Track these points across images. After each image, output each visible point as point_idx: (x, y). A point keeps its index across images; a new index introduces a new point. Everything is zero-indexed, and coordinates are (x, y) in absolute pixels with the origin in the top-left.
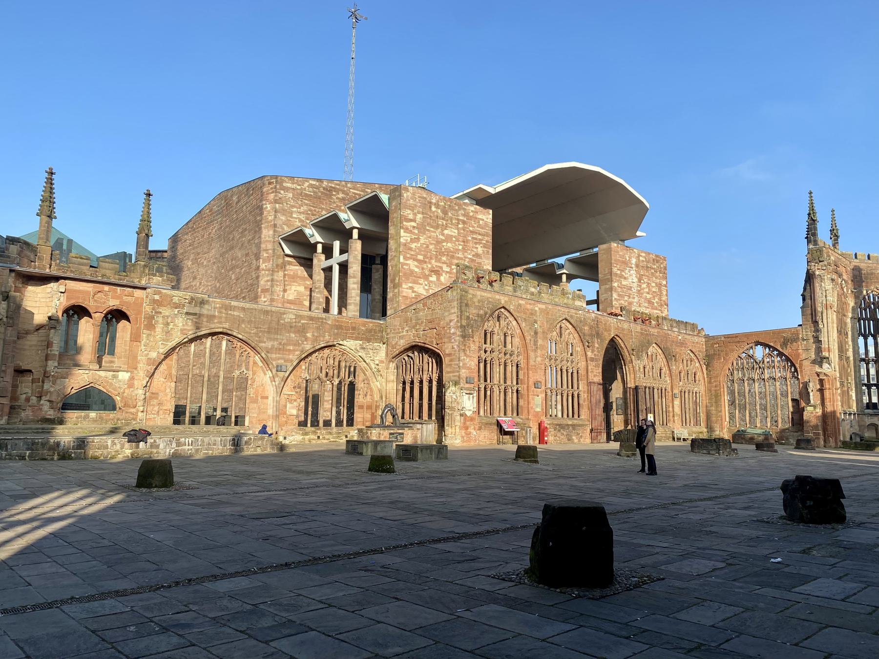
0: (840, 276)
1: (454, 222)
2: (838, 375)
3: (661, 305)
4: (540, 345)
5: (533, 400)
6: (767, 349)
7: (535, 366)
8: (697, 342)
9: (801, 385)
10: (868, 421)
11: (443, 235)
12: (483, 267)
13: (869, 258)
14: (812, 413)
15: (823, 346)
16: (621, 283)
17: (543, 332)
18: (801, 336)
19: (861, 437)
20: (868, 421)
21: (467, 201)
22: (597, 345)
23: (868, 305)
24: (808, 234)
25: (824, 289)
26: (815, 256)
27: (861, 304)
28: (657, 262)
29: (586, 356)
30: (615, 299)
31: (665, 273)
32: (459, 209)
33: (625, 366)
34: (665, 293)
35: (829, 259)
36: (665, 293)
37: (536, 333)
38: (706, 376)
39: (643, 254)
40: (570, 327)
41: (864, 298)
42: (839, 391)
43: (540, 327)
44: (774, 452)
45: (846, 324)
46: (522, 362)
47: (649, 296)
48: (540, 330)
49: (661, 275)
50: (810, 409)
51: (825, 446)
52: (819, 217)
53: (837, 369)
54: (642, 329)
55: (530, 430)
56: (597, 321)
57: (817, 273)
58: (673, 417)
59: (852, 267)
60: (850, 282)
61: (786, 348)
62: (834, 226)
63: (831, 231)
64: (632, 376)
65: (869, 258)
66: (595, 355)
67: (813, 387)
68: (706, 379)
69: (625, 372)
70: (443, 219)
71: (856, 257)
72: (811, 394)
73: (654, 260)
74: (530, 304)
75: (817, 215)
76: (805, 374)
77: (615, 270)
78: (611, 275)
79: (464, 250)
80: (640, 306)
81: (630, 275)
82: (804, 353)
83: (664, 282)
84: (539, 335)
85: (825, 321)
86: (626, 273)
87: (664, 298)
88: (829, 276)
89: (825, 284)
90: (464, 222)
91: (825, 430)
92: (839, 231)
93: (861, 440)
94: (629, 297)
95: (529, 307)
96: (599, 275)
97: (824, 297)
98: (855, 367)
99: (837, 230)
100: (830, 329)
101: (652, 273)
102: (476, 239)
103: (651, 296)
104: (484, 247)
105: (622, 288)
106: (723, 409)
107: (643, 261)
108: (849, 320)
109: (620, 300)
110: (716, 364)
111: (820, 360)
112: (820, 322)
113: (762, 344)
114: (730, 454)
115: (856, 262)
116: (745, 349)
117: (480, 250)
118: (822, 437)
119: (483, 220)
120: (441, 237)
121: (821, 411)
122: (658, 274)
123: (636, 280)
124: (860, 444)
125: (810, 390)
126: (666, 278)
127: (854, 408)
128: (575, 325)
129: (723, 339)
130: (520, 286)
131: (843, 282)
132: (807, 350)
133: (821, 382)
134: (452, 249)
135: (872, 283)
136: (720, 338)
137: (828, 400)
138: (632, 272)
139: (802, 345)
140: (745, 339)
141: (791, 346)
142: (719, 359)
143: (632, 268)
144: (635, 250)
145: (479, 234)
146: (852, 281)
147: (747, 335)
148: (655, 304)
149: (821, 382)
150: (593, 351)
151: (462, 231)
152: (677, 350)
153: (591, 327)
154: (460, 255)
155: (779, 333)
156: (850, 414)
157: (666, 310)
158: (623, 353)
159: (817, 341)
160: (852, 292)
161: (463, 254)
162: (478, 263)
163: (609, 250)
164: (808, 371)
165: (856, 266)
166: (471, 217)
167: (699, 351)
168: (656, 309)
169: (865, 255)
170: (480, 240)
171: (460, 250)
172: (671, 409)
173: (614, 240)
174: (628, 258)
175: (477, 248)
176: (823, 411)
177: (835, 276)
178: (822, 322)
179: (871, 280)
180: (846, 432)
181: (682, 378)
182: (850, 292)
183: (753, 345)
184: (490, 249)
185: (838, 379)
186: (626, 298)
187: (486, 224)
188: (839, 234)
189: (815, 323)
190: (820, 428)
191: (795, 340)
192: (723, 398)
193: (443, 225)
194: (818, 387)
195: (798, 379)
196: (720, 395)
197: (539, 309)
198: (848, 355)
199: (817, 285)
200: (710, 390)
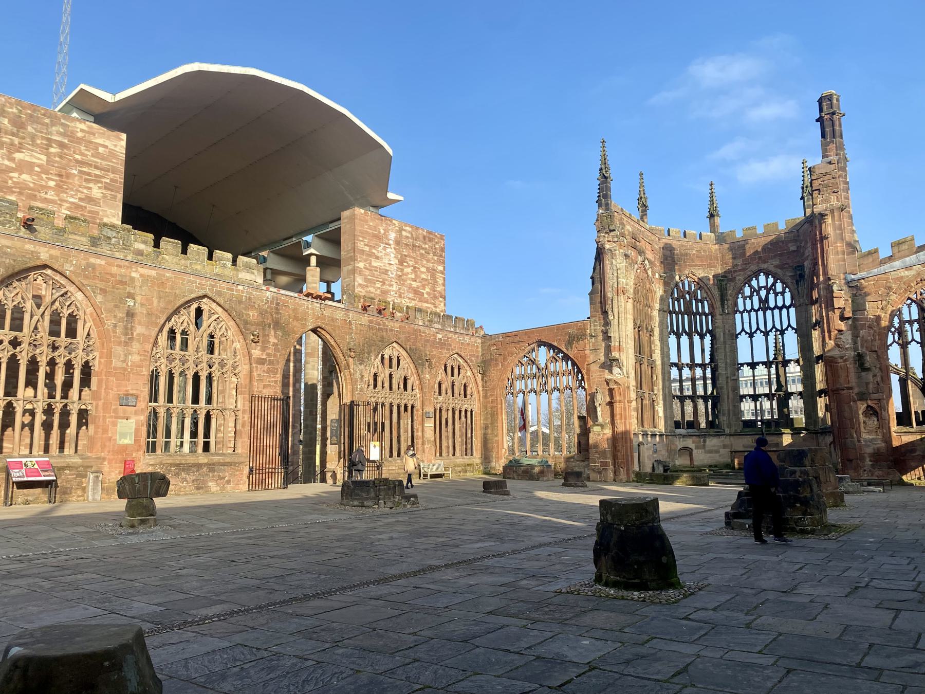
0: (641, 252)
1: (39, 142)
2: (633, 383)
3: (435, 297)
4: (138, 335)
5: (115, 424)
6: (552, 351)
7: (125, 369)
8: (468, 344)
9: (589, 397)
10: (680, 444)
11: (12, 160)
12: (102, 219)
13: (685, 236)
14: (600, 434)
15: (612, 344)
16: (370, 263)
17: (149, 314)
18: (588, 331)
19: (664, 466)
20: (680, 444)
21: (75, 115)
22: (273, 340)
23: (681, 294)
24: (599, 196)
25: (615, 268)
26: (605, 224)
27: (672, 294)
28: (430, 241)
29: (250, 355)
30: (360, 285)
31: (441, 256)
32: (53, 124)
33: (340, 373)
34: (440, 281)
35: (623, 228)
36: (440, 281)
37: (130, 314)
38: (481, 389)
39: (408, 228)
40: (219, 309)
41: (677, 285)
42: (634, 404)
43: (142, 305)
44: (505, 495)
45: (651, 318)
46: (96, 362)
47: (414, 284)
48: (139, 309)
49: (436, 258)
50: (596, 429)
51: (615, 480)
52: (613, 173)
53: (632, 375)
54: (370, 322)
55: (97, 477)
56: (278, 304)
57: (607, 246)
58: (423, 444)
59: (662, 245)
60: (658, 264)
61: (571, 348)
62: (642, 193)
63: (638, 200)
64: (349, 387)
65: (685, 236)
66: (268, 354)
67: (601, 399)
68: (481, 393)
69: (341, 383)
70: (13, 134)
71: (669, 235)
72: (599, 409)
73: (424, 237)
74: (119, 266)
75: (610, 171)
76: (593, 383)
77: (360, 245)
78: (354, 252)
79: (59, 188)
80: (400, 296)
81: (386, 254)
82: (594, 355)
83: (440, 268)
84: (136, 319)
85: (615, 310)
86: (380, 251)
87: (439, 288)
88: (621, 251)
89: (616, 261)
90: (61, 145)
91: (615, 458)
92: (648, 200)
93: (665, 471)
94: (384, 283)
95: (114, 270)
96: (342, 253)
97: (615, 278)
98: (663, 374)
99: (646, 198)
100: (622, 320)
101: (422, 254)
102: (89, 174)
103: (419, 284)
104: (106, 188)
105: (371, 270)
106: (500, 432)
107: (407, 237)
108: (656, 314)
109: (367, 287)
110: (494, 373)
111: (610, 363)
112: (610, 313)
113: (550, 346)
114: (397, 504)
115: (666, 240)
116: (527, 351)
117: (96, 192)
118: (611, 467)
119: (105, 147)
120: (6, 162)
121: (611, 431)
122: (431, 256)
123: (395, 261)
124: (658, 476)
125: (597, 404)
126: (444, 263)
127: (661, 427)
128: (227, 307)
129: (501, 339)
130: (109, 238)
131: (646, 262)
132: (596, 350)
133: (611, 391)
134: (31, 185)
135: (686, 266)
136: (498, 338)
137: (618, 416)
138: (388, 250)
139: (589, 343)
140: (525, 338)
141: (577, 346)
142: (497, 365)
143: (390, 245)
144: (394, 221)
145: (96, 167)
146: (662, 262)
147: (528, 333)
148: (426, 296)
149: (611, 391)
150: (264, 349)
151: (57, 159)
152: (434, 353)
153: (262, 313)
154: (51, 195)
155: (564, 329)
156: (654, 435)
157: (442, 304)
158: (335, 355)
159: (607, 338)
160: (661, 276)
161: (58, 195)
162: (90, 212)
163: (353, 218)
164: (597, 375)
165: (666, 244)
166: (78, 138)
167: (471, 355)
168: (427, 302)
169: (679, 231)
170: (96, 176)
171: (50, 187)
172: (420, 434)
173: (362, 206)
174: (382, 231)
175: (90, 188)
176: (613, 431)
177: (632, 253)
178: (612, 311)
179: (685, 262)
180: (647, 460)
181: (443, 391)
182: (657, 276)
183: (535, 345)
184: (118, 192)
185: (632, 388)
186: (378, 285)
187: (112, 154)
188: (648, 203)
189: (605, 313)
190: (609, 455)
191: (581, 338)
192: (500, 418)
193: (12, 144)
194: (608, 399)
195: (585, 389)
196: (497, 414)
197: (141, 275)
198: (653, 359)
199: (607, 262)
200: (486, 408)
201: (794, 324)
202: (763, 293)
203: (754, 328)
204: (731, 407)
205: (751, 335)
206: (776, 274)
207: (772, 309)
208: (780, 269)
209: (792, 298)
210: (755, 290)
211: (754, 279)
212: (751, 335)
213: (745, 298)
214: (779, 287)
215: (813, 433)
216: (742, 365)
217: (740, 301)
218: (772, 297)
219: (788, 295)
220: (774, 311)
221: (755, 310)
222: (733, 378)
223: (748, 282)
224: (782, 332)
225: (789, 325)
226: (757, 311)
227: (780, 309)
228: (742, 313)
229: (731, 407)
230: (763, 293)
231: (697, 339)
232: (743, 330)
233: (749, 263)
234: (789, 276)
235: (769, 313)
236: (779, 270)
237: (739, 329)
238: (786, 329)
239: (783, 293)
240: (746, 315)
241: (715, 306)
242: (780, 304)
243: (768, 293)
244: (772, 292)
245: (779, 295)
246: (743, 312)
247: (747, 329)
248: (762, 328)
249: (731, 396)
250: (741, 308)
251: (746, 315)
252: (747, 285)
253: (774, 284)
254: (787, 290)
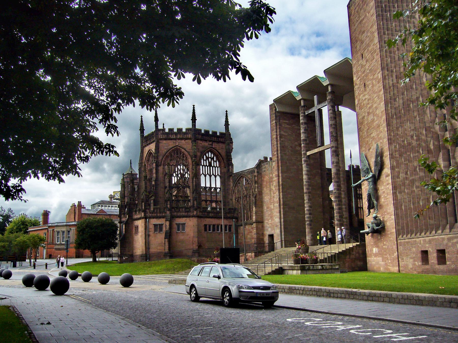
202: (210, 160)
209: (219, 164)
213: (204, 160)
218: (212, 162)
224: (215, 176)
225: (218, 174)
230: (210, 160)
232: (203, 173)
237: (201, 173)
239: (216, 162)
247: (204, 174)
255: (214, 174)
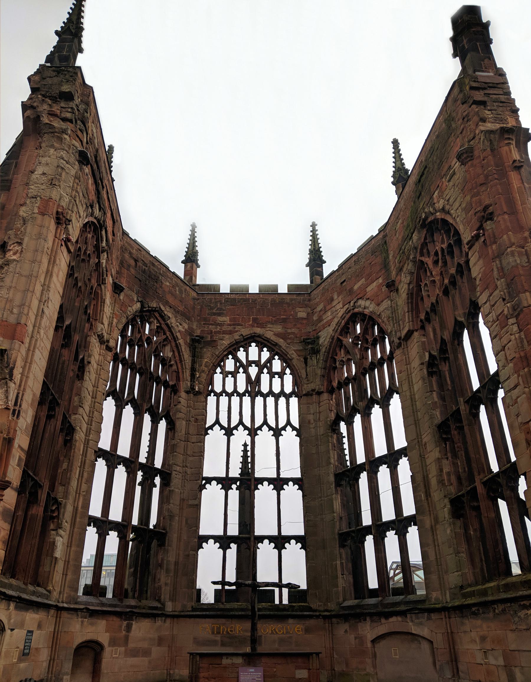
201: (295, 421)
202: (253, 371)
203: (235, 421)
204: (181, 559)
205: (229, 432)
206: (276, 344)
207: (265, 396)
208: (283, 339)
209: (295, 383)
210: (242, 365)
211: (242, 349)
212: (229, 432)
213: (225, 374)
214: (277, 365)
215: (325, 617)
216: (209, 480)
217: (218, 378)
218: (265, 378)
219: (288, 379)
220: (268, 398)
221: (239, 394)
222: (191, 502)
223: (232, 351)
224: (277, 432)
225: (289, 423)
226: (241, 396)
227: (277, 397)
228: (218, 395)
229: (181, 559)
230: (253, 371)
231: (147, 418)
232: (217, 422)
233: (239, 325)
234: (294, 350)
235: (259, 400)
236: (281, 340)
237: (210, 420)
238: (284, 428)
239: (281, 375)
240: (224, 400)
241: (181, 376)
242: (277, 389)
243: (260, 372)
244: (265, 371)
245: (276, 376)
246: (221, 394)
248: (247, 422)
249: (185, 537)
250: (218, 388)
251: (224, 400)
252: (230, 357)
253: (270, 360)
254: (288, 371)
255: (272, 422)
